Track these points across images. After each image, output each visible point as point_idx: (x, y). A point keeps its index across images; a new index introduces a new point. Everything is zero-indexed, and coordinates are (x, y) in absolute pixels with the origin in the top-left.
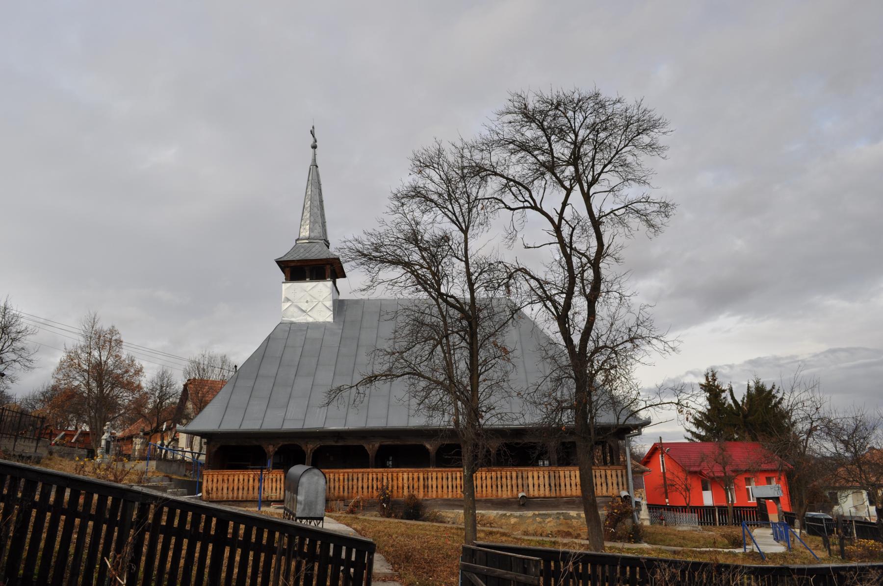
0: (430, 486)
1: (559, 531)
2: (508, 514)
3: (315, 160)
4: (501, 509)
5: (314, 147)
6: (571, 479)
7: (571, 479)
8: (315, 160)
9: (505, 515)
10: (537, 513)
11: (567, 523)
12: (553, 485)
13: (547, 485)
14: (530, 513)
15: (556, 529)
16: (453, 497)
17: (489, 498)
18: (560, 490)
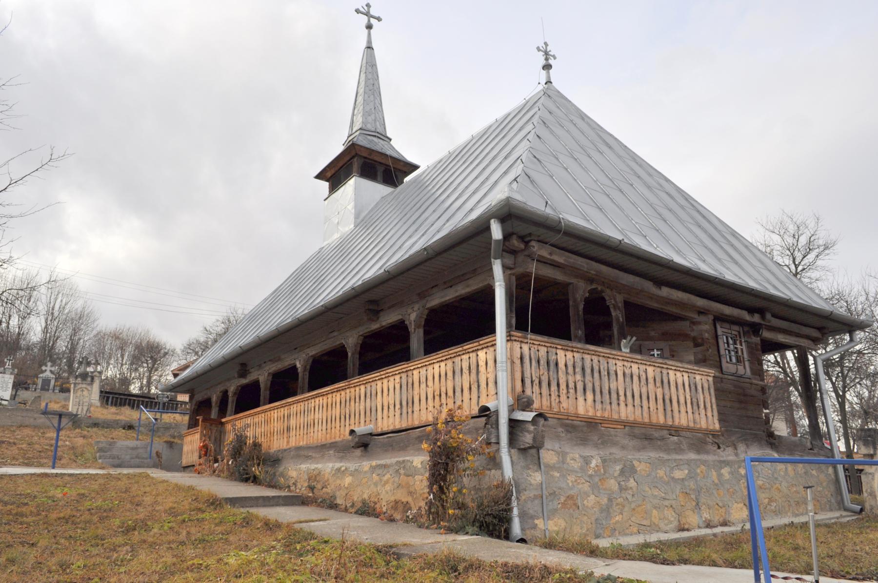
0: (291, 427)
1: (396, 502)
2: (343, 469)
3: (369, 41)
4: (341, 459)
5: (369, 27)
6: (427, 386)
7: (427, 386)
8: (369, 41)
9: (339, 470)
10: (374, 463)
11: (408, 486)
12: (404, 403)
13: (398, 406)
14: (366, 465)
15: (393, 499)
16: (307, 442)
17: (337, 439)
18: (413, 412)
